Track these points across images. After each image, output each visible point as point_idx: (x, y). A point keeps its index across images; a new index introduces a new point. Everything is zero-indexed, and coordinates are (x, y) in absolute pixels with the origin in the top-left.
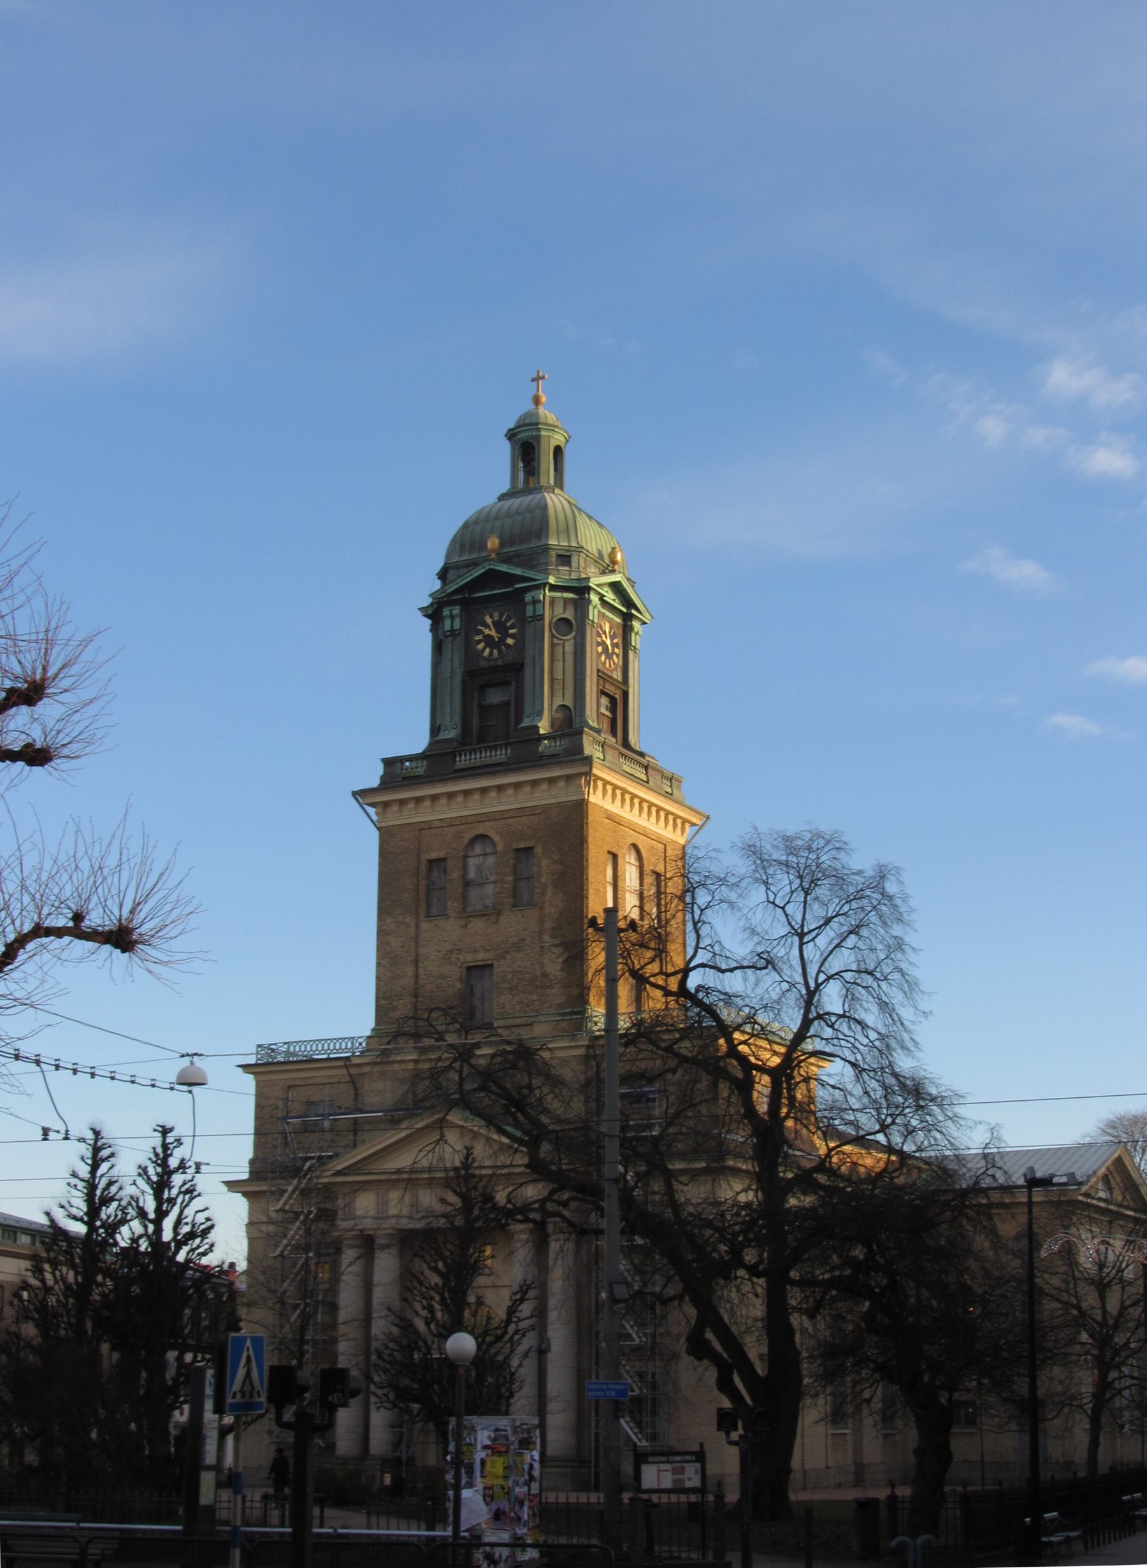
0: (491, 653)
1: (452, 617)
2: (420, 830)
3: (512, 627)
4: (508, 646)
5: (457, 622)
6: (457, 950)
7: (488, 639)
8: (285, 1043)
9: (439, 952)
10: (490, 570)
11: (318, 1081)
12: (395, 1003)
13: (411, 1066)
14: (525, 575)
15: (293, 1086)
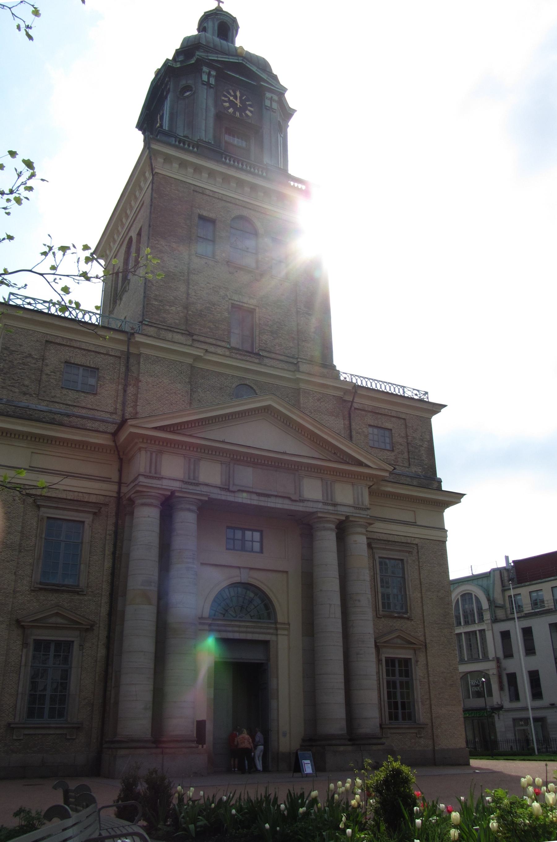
0: (234, 112)
1: (209, 75)
2: (193, 190)
3: (250, 106)
4: (247, 115)
5: (212, 81)
6: (225, 288)
7: (232, 104)
8: (45, 302)
9: (208, 283)
10: (242, 63)
11: (84, 346)
12: (168, 308)
13: (190, 361)
14: (268, 80)
15: (51, 342)
